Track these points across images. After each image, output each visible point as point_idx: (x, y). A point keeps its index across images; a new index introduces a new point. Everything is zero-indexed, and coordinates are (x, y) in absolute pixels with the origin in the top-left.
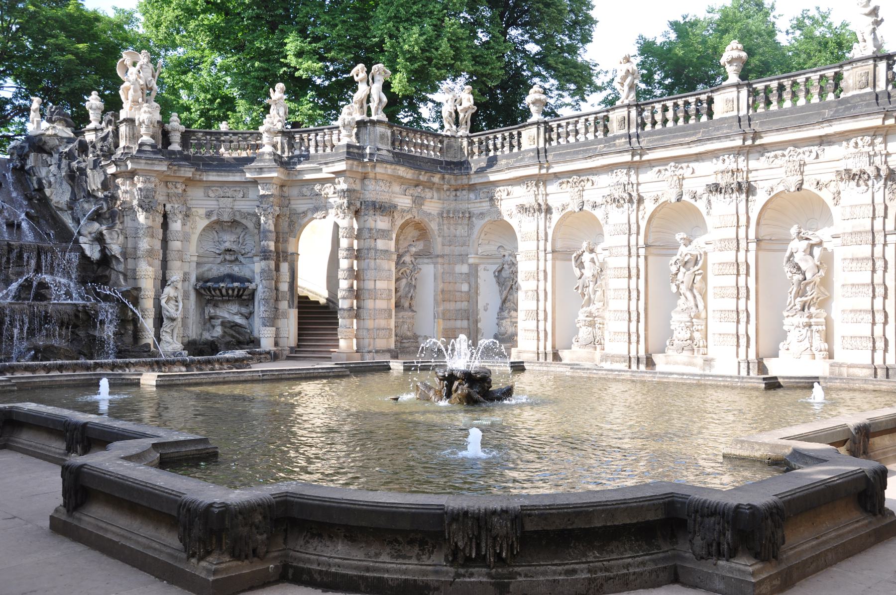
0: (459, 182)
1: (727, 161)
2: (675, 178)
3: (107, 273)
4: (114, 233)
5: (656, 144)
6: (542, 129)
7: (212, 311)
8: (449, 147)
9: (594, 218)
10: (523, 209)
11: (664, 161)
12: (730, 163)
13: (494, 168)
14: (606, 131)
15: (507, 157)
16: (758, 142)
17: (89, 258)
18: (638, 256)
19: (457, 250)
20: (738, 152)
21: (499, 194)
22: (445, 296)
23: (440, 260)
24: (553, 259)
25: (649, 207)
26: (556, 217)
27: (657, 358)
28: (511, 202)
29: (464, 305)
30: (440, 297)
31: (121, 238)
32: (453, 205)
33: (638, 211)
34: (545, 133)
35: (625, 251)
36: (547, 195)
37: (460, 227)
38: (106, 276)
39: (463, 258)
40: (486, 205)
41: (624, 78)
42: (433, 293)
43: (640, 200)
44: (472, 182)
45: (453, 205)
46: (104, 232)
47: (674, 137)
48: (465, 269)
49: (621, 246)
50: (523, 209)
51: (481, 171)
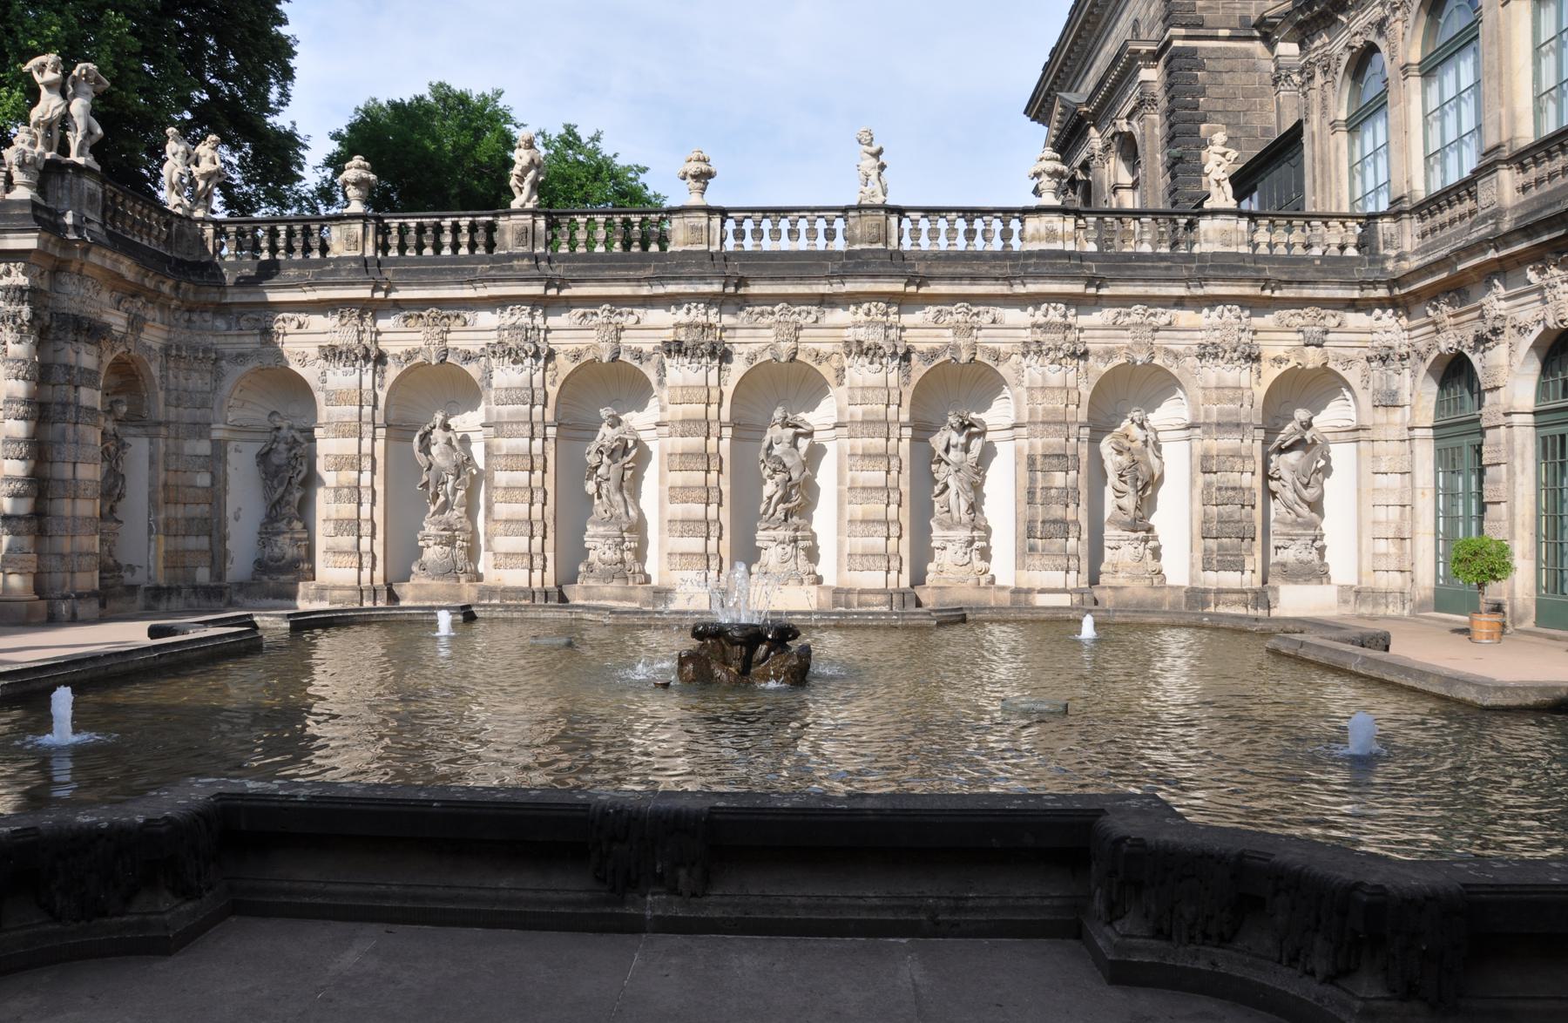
0: (203, 298)
1: (694, 312)
2: (611, 328)
5: (575, 275)
6: (371, 228)
8: (181, 234)
9: (467, 377)
10: (332, 353)
11: (594, 301)
12: (697, 314)
13: (275, 281)
14: (490, 246)
15: (297, 265)
16: (742, 291)
18: (545, 439)
19: (187, 414)
20: (710, 300)
21: (281, 324)
22: (166, 494)
23: (163, 431)
24: (387, 438)
25: (565, 366)
26: (392, 372)
27: (569, 591)
28: (303, 341)
29: (202, 510)
30: (161, 496)
32: (182, 336)
33: (545, 370)
34: (376, 234)
35: (526, 429)
36: (378, 333)
37: (195, 375)
39: (200, 429)
40: (251, 342)
41: (525, 170)
42: (145, 490)
43: (551, 355)
44: (228, 300)
45: (182, 336)
47: (609, 268)
48: (204, 447)
49: (518, 423)
50: (332, 353)
51: (244, 283)
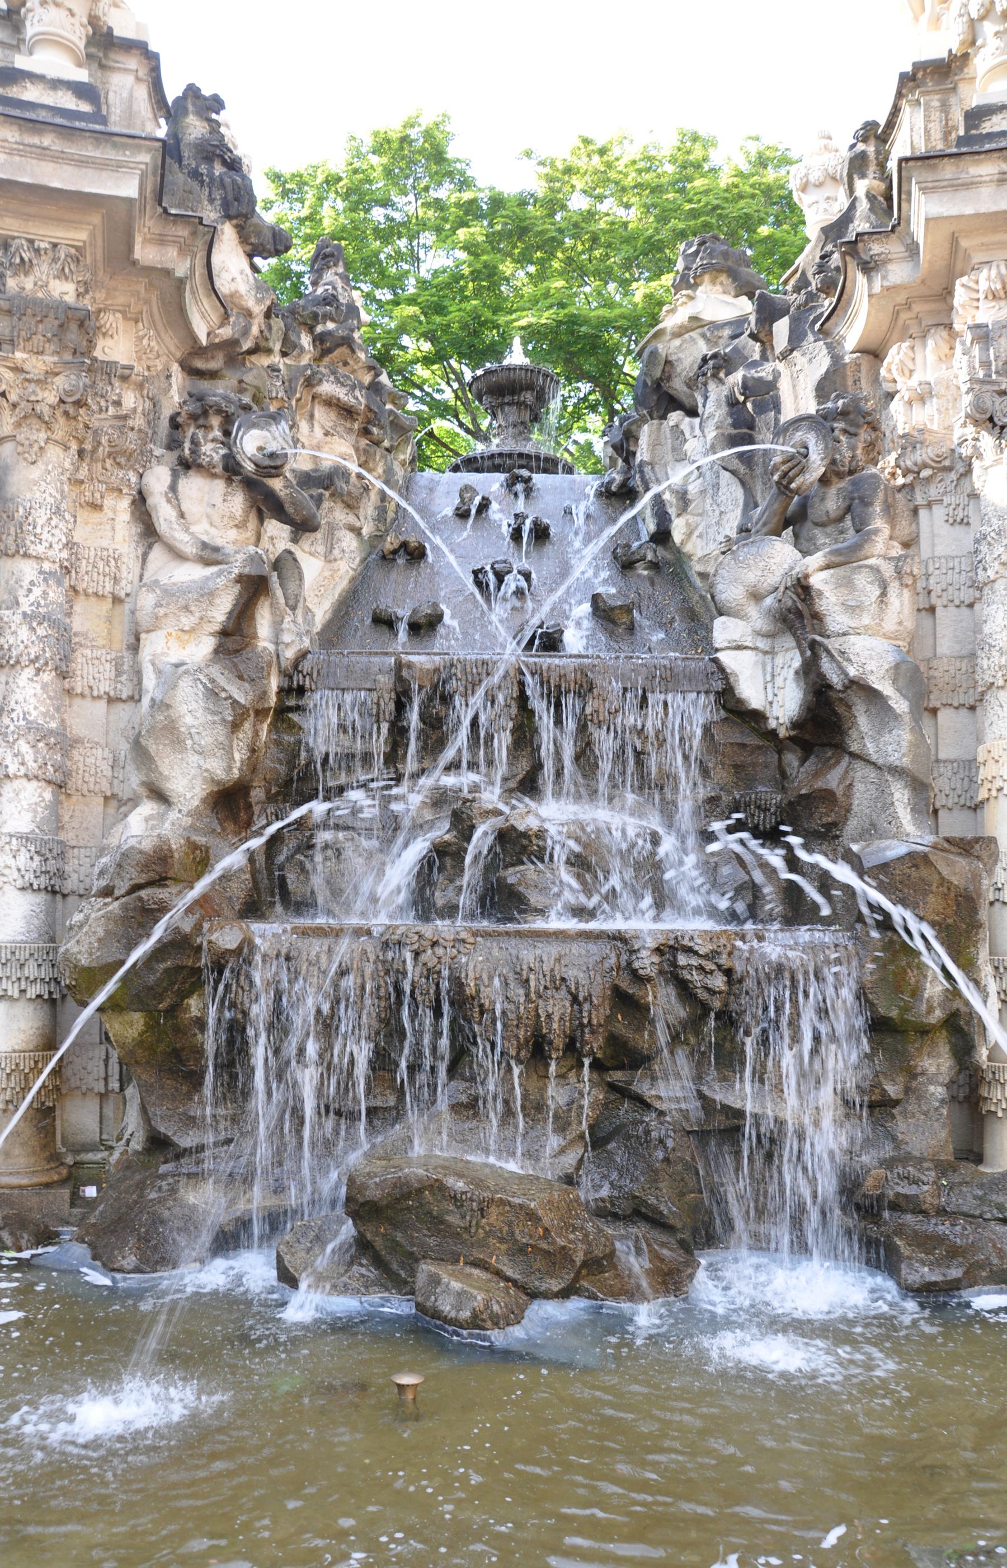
3: (832, 780)
17: (757, 717)
31: (900, 604)
38: (827, 796)
46: (817, 581)
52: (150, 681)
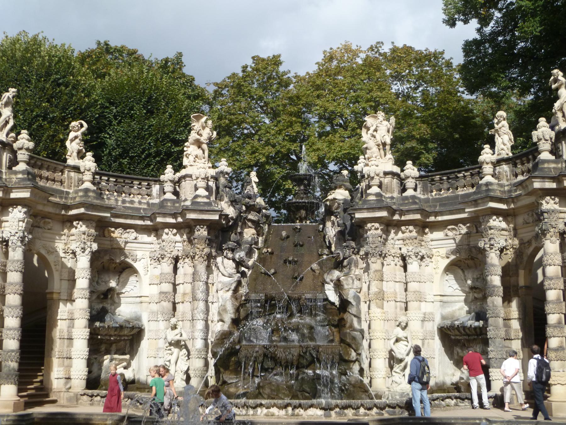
4: (350, 279)
7: (460, 351)
52: (220, 300)
